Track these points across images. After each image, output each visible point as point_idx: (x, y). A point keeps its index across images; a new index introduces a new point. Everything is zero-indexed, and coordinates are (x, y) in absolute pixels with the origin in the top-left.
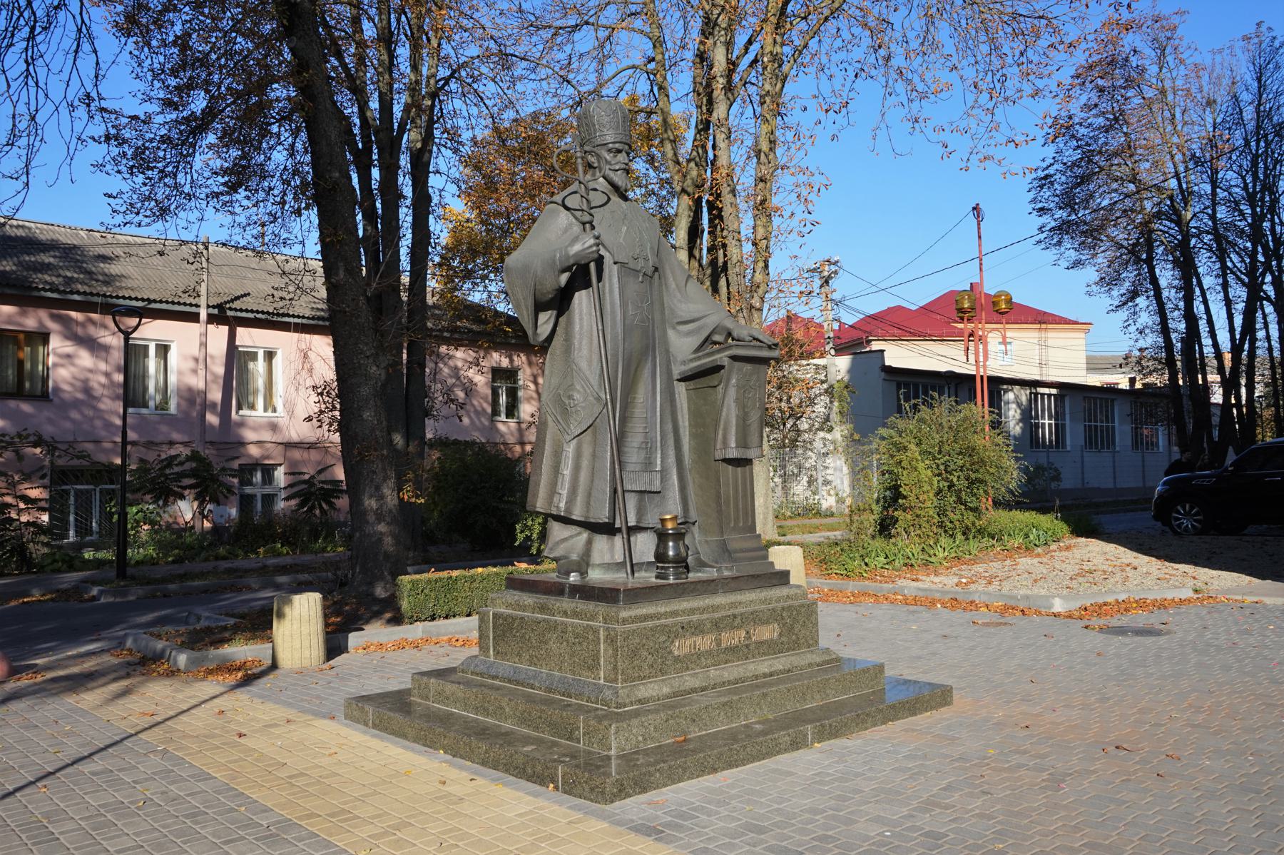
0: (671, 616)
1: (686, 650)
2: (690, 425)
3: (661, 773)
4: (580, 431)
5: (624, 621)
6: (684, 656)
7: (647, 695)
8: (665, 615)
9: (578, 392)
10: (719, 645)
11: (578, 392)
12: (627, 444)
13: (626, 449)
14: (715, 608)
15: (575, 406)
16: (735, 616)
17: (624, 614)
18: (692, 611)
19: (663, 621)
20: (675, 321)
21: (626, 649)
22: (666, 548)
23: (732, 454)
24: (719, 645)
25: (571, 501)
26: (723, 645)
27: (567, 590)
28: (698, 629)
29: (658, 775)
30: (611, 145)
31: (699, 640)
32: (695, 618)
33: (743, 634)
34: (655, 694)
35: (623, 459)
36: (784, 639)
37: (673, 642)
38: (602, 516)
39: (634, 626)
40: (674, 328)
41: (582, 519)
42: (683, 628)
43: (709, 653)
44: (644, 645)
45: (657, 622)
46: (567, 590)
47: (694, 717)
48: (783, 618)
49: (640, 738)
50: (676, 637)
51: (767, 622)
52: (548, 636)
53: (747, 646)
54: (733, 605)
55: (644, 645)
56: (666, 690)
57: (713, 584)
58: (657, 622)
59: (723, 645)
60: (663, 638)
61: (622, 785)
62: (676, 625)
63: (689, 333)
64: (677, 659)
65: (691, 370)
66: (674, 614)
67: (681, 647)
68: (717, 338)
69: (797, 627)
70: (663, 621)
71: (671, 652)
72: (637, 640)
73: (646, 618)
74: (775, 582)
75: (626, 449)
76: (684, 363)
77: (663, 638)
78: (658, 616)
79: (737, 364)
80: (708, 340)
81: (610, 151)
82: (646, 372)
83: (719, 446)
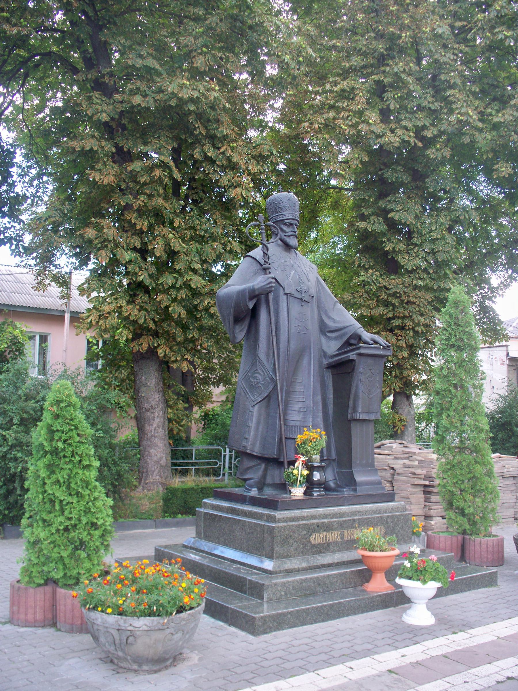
0: (311, 519)
1: (319, 541)
2: (334, 397)
3: (291, 615)
4: (260, 400)
5: (280, 521)
6: (319, 544)
7: (291, 567)
9: (260, 374)
10: (342, 538)
11: (260, 374)
12: (290, 408)
13: (290, 412)
14: (342, 515)
15: (258, 383)
16: (354, 520)
17: (279, 514)
18: (325, 516)
19: (304, 522)
20: (326, 330)
21: (279, 538)
24: (342, 538)
25: (254, 444)
26: (345, 539)
27: (248, 499)
28: (328, 528)
29: (289, 616)
30: (286, 221)
31: (329, 535)
32: (326, 521)
34: (296, 567)
35: (288, 418)
37: (311, 535)
38: (273, 453)
39: (285, 524)
40: (326, 335)
41: (260, 455)
42: (318, 526)
43: (336, 543)
44: (291, 536)
45: (301, 522)
46: (248, 499)
47: (320, 582)
48: (387, 523)
49: (283, 593)
50: (313, 532)
52: (235, 527)
54: (354, 513)
55: (291, 536)
56: (304, 565)
58: (301, 522)
59: (345, 539)
60: (304, 532)
61: (265, 621)
62: (313, 524)
63: (336, 338)
64: (314, 546)
65: (334, 362)
66: (313, 517)
67: (317, 538)
68: (352, 341)
70: (304, 522)
71: (310, 542)
72: (287, 532)
73: (293, 519)
75: (290, 412)
76: (332, 357)
77: (304, 532)
78: (304, 518)
79: (363, 359)
80: (348, 343)
81: (285, 224)
82: (305, 362)
83: (350, 411)
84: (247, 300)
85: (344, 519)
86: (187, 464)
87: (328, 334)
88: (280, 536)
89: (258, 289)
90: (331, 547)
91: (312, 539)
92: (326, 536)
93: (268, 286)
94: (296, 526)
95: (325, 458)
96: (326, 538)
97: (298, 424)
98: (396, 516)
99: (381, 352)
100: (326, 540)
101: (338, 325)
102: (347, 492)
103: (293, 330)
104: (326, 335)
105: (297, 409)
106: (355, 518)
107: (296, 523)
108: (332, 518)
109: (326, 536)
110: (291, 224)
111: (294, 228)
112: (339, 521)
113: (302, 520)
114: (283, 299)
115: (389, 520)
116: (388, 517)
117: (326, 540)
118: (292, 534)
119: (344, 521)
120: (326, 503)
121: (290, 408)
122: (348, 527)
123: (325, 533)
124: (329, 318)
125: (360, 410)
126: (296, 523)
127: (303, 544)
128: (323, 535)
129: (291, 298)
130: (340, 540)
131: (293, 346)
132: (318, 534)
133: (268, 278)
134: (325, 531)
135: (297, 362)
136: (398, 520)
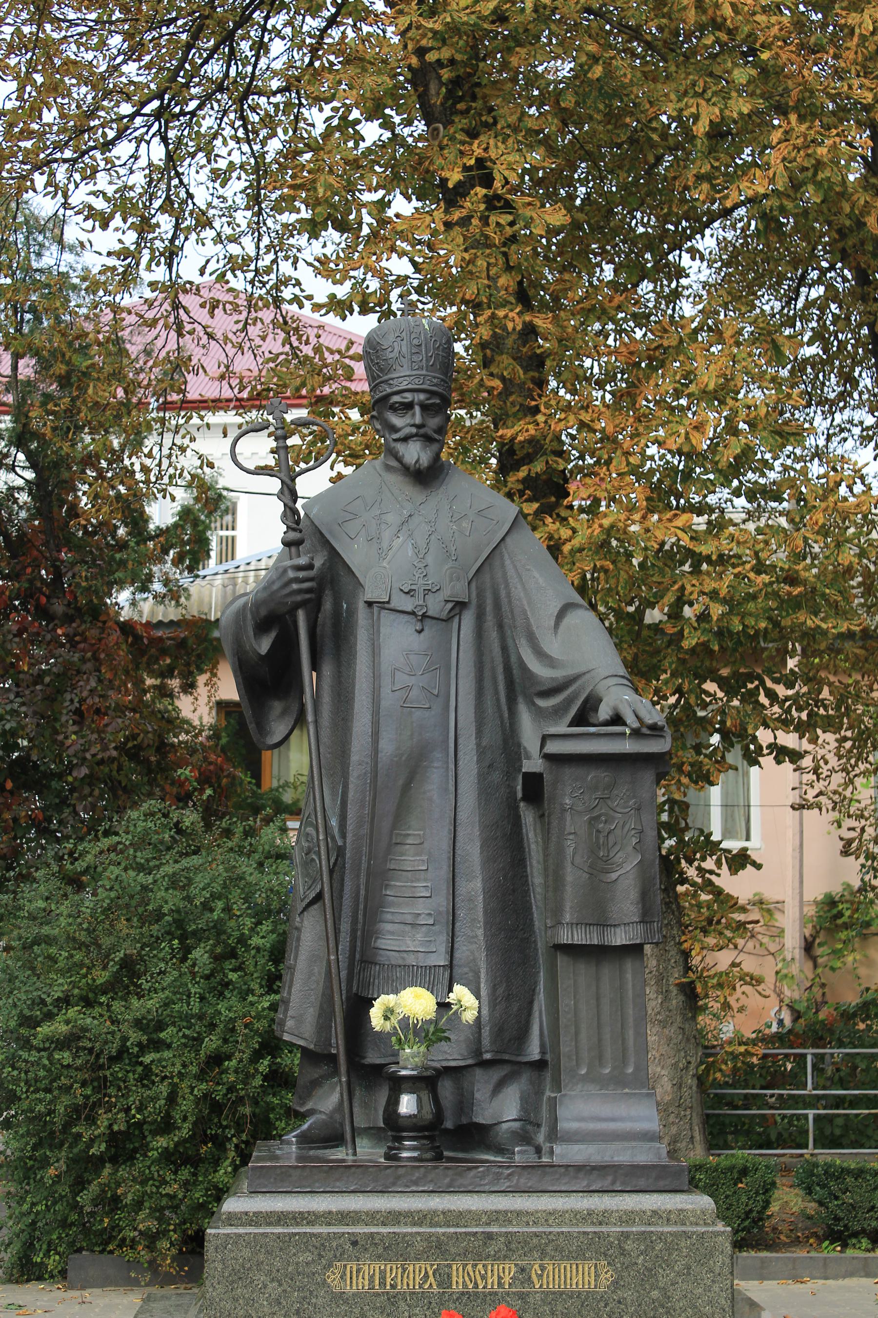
8: (328, 1218)
10: (445, 1280)
16: (490, 1236)
18: (394, 1217)
21: (220, 1267)
22: (397, 1102)
23: (565, 937)
26: (457, 1286)
30: (396, 398)
31: (392, 1270)
33: (508, 1271)
36: (628, 1295)
37: (330, 1265)
42: (355, 1243)
44: (259, 1264)
48: (623, 1253)
51: (579, 1255)
53: (522, 1296)
54: (497, 1216)
55: (259, 1264)
57: (472, 1173)
69: (665, 1276)
72: (247, 1253)
73: (281, 1218)
74: (642, 1183)
81: (393, 408)
84: (251, 633)
85: (452, 1230)
86: (839, 1102)
87: (542, 703)
88: (223, 1261)
89: (264, 602)
90: (402, 1304)
91: (333, 1278)
92: (383, 1273)
93: (287, 591)
94: (278, 1236)
95: (487, 1056)
96: (383, 1279)
97: (411, 960)
98: (661, 1236)
99: (628, 746)
100: (383, 1283)
101: (558, 674)
102: (521, 1155)
103: (388, 700)
104: (534, 704)
105: (409, 919)
106: (494, 1229)
107: (279, 1230)
108: (414, 1224)
109: (383, 1273)
110: (408, 407)
111: (414, 415)
112: (431, 1235)
113: (310, 1223)
114: (362, 615)
115: (629, 1246)
116: (626, 1236)
117: (383, 1283)
118: (261, 1257)
119: (450, 1236)
120: (416, 1183)
121: (389, 917)
122: (464, 1255)
123: (377, 1266)
124: (540, 654)
125: (567, 917)
126: (279, 1230)
127: (300, 1289)
128: (371, 1268)
129: (384, 613)
130: (435, 1289)
131: (387, 747)
132: (352, 1266)
133: (285, 571)
134: (379, 1257)
135: (406, 788)
136: (669, 1249)
